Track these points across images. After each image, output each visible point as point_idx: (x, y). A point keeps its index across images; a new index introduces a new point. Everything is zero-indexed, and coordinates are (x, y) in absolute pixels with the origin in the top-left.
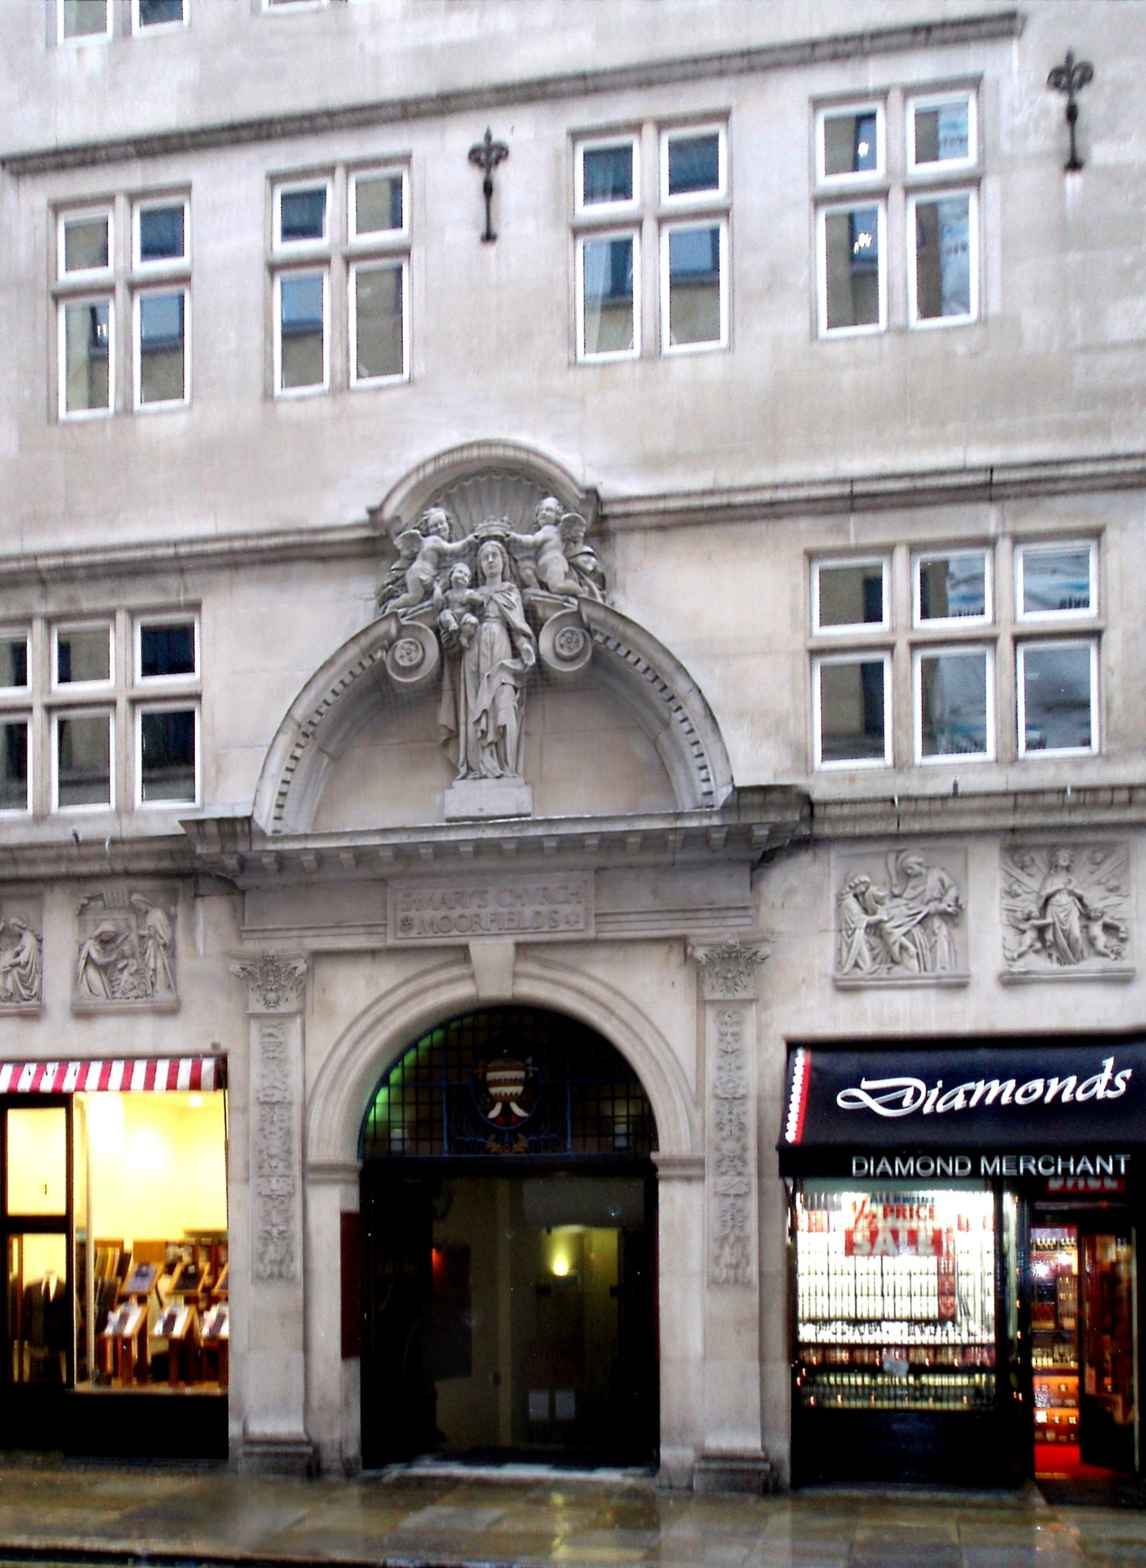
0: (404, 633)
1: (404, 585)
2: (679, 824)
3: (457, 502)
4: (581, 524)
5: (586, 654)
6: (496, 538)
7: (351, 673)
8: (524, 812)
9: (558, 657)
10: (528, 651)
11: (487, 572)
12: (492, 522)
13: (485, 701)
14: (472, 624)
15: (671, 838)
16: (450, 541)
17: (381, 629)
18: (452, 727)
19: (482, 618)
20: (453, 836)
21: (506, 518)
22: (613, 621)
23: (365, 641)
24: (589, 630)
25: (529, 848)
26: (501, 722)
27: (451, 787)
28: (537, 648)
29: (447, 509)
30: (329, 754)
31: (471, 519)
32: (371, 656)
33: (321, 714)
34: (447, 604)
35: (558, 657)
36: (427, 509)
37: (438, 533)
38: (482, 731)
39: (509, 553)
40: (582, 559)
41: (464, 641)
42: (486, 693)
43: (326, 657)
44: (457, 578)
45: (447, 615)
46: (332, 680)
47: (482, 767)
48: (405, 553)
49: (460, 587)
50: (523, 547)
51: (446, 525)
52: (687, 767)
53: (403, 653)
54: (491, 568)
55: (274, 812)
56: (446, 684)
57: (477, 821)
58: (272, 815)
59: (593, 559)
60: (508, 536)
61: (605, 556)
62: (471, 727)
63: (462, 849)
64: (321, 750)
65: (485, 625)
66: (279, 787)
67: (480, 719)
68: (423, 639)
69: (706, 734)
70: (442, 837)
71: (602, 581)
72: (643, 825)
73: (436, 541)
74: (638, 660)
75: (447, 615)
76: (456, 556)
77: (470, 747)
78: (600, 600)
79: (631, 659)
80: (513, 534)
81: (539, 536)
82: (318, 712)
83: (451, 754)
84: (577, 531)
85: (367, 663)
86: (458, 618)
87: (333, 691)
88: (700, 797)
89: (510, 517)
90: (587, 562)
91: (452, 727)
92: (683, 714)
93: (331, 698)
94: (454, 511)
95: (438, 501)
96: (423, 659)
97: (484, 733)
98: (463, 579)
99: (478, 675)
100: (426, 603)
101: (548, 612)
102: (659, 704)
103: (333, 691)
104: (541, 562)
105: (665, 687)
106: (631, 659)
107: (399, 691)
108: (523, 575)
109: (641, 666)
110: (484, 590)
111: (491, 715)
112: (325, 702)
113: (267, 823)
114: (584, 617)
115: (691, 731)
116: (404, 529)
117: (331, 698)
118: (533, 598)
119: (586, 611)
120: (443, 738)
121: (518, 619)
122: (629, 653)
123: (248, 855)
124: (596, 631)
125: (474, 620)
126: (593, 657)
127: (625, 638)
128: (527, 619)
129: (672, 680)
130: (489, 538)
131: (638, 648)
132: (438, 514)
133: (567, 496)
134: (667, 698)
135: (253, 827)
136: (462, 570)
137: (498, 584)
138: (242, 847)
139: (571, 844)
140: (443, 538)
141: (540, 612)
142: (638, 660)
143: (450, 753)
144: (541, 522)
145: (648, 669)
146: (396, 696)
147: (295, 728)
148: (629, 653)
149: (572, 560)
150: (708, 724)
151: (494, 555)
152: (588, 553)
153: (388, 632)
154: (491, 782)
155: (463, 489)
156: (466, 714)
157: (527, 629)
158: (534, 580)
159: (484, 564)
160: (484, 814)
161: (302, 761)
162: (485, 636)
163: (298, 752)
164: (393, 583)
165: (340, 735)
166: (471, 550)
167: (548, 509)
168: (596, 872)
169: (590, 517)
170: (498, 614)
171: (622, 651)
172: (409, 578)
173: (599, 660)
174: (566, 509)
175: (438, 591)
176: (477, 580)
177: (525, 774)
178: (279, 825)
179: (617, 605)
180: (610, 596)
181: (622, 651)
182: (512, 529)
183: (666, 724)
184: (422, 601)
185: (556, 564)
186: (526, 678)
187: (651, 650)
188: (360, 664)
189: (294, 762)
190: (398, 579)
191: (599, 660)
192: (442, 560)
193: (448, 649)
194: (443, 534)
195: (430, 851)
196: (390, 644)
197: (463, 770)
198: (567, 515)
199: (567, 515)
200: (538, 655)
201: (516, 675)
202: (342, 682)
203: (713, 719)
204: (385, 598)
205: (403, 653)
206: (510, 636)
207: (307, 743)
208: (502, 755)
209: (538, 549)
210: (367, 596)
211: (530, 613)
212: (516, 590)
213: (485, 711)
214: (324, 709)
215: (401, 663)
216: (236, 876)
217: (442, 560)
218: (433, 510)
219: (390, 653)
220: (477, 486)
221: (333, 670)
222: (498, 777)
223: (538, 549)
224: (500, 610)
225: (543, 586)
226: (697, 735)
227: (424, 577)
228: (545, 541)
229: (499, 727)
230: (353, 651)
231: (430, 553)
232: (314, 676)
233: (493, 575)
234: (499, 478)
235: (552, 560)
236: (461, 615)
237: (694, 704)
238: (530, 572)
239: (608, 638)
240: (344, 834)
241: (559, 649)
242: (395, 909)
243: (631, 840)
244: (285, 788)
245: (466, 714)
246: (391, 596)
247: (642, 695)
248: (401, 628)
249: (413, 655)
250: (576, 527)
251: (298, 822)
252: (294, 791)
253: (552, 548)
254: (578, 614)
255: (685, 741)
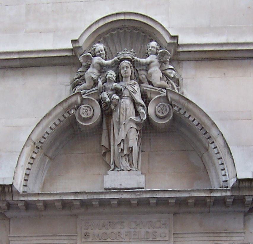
0: (84, 102)
1: (84, 79)
2: (212, 195)
3: (109, 41)
4: (168, 55)
5: (170, 116)
6: (128, 59)
7: (59, 119)
8: (141, 187)
9: (157, 116)
10: (143, 113)
11: (123, 75)
12: (125, 52)
13: (123, 135)
14: (117, 99)
15: (208, 201)
16: (106, 60)
17: (73, 99)
18: (107, 146)
19: (121, 97)
20: (108, 197)
21: (132, 50)
22: (183, 101)
23: (65, 105)
24: (171, 105)
25: (143, 203)
26: (130, 145)
27: (107, 174)
28: (147, 112)
29: (104, 44)
30: (49, 157)
31: (116, 50)
32: (68, 112)
33: (45, 138)
34: (104, 89)
35: (157, 116)
36: (95, 44)
37: (100, 55)
38: (122, 149)
39: (134, 67)
40: (168, 71)
41: (113, 107)
42: (123, 131)
43: (47, 112)
44: (109, 77)
45: (105, 95)
46: (50, 122)
47: (121, 165)
48: (84, 64)
49: (110, 81)
50: (141, 64)
51: (104, 52)
52: (216, 169)
53: (84, 111)
54: (125, 73)
55: (23, 183)
56: (104, 127)
57: (119, 190)
58: (22, 184)
59: (174, 72)
60: (133, 59)
61: (179, 70)
62: (116, 147)
63: (112, 203)
64: (45, 155)
65: (123, 100)
66: (26, 171)
67: (120, 143)
68: (93, 105)
69: (225, 155)
70: (103, 197)
71: (178, 82)
72: (196, 195)
73: (99, 59)
74: (194, 120)
75: (105, 95)
76: (109, 67)
77: (116, 156)
78: (177, 91)
79: (191, 119)
80: (136, 58)
81: (148, 59)
82: (43, 137)
83: (107, 159)
84: (166, 58)
85: (67, 115)
86: (110, 96)
87: (51, 128)
88: (222, 183)
89: (134, 50)
90: (171, 73)
91: (107, 146)
92: (214, 145)
93: (49, 131)
94: (108, 46)
95: (100, 40)
96: (93, 114)
97: (122, 150)
98: (112, 78)
99: (119, 123)
100: (95, 89)
101: (152, 96)
102: (204, 140)
103: (51, 128)
104: (149, 72)
105: (207, 132)
106: (191, 119)
107: (82, 129)
108: (141, 77)
109: (196, 122)
110: (122, 83)
111: (125, 142)
112: (47, 132)
113: (20, 188)
114: (169, 98)
115: (218, 153)
116: (84, 53)
117: (49, 131)
118: (145, 89)
119: (170, 96)
120: (103, 151)
121: (138, 98)
122: (190, 116)
123: (11, 202)
124: (175, 105)
125: (117, 97)
126: (173, 117)
127: (188, 109)
128: (142, 98)
129: (210, 130)
130: (125, 59)
131: (195, 114)
132: (100, 47)
133: (162, 41)
134: (207, 137)
135: (13, 189)
136: (111, 74)
137: (129, 81)
138: (8, 198)
139: (163, 202)
140: (102, 58)
141: (149, 95)
142: (194, 120)
143: (105, 158)
144: (149, 53)
145: (199, 124)
146: (81, 131)
147: (32, 144)
148: (190, 116)
149: (163, 72)
150: (226, 150)
151: (127, 67)
152: (171, 69)
153: (76, 101)
154: (125, 173)
155: (112, 35)
156: (114, 141)
157: (143, 103)
158: (146, 80)
159: (122, 71)
160: (122, 187)
161: (36, 160)
162: (123, 105)
163: (34, 156)
164: (78, 78)
165: (54, 148)
166: (116, 65)
167: (152, 47)
168: (174, 214)
169: (172, 52)
170: (129, 95)
171: (187, 115)
172: (86, 76)
173: (176, 118)
174: (161, 47)
175: (100, 83)
176: (119, 79)
177: (141, 169)
178: (25, 189)
179: (184, 93)
180: (182, 89)
181: (187, 115)
182: (135, 56)
183: (207, 149)
184: (92, 88)
185: (156, 73)
186: (142, 126)
187: (200, 115)
188: (63, 115)
189: (32, 160)
190: (81, 76)
191: (176, 118)
192: (102, 69)
193: (105, 111)
194: (103, 56)
195: (97, 203)
196: (78, 107)
197: (113, 167)
198: (162, 50)
199: (162, 50)
200: (147, 115)
201: (137, 124)
202: (55, 123)
203: (228, 148)
204: (75, 85)
205: (84, 111)
206: (135, 106)
207: (38, 151)
208: (131, 161)
209: (148, 66)
210: (66, 84)
211: (144, 95)
212: (137, 84)
213: (123, 140)
214: (46, 136)
215: (83, 116)
216: (5, 212)
217: (102, 69)
218: (98, 44)
219: (77, 111)
220: (118, 34)
221: (51, 118)
222: (129, 171)
223: (148, 66)
224: (130, 93)
225: (150, 83)
226: (221, 155)
227: (93, 76)
228: (151, 62)
229: (129, 147)
230: (60, 109)
231: (96, 65)
232: (41, 120)
233: (126, 77)
234: (129, 31)
235: (154, 71)
236: (111, 95)
237: (220, 141)
238: (144, 76)
239: (180, 109)
240: (57, 194)
241: (157, 113)
242: (81, 228)
243: (190, 201)
244: (28, 172)
245: (114, 141)
246: (78, 84)
247: (195, 135)
248: (82, 100)
249: (89, 112)
250: (166, 56)
251: (35, 187)
252: (32, 173)
253: (154, 66)
254: (167, 97)
255: (215, 157)
